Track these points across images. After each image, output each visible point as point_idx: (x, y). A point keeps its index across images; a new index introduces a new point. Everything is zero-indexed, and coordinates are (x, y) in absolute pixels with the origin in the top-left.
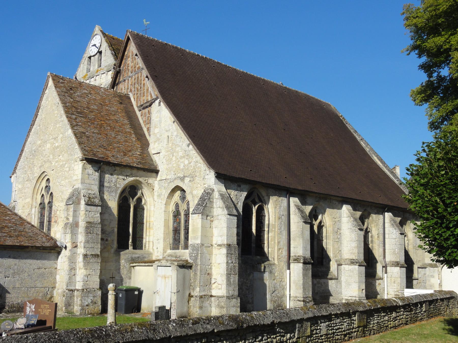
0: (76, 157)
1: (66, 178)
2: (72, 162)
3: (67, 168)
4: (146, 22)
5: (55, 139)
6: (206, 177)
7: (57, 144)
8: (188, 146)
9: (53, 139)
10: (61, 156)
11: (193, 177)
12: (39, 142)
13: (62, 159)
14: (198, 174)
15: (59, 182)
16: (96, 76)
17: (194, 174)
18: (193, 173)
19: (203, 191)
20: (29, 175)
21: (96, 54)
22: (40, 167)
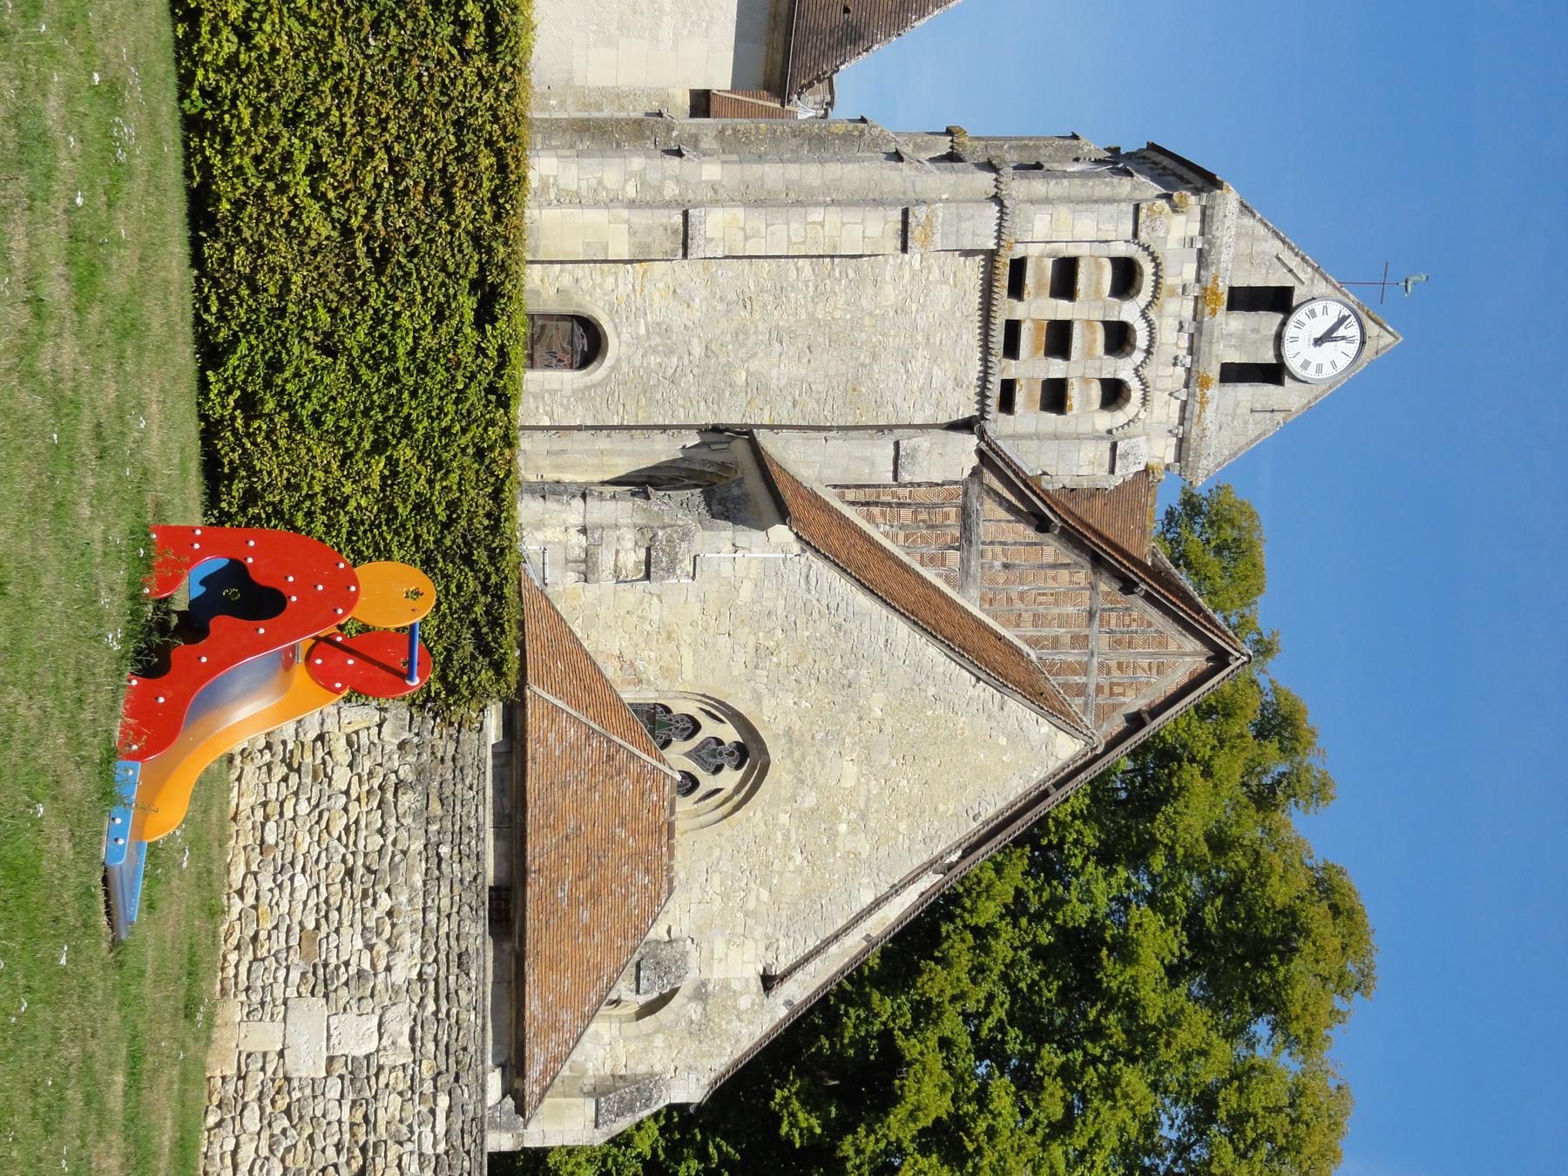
0: (782, 944)
1: (725, 897)
2: (770, 930)
3: (758, 898)
4: (1415, 284)
5: (863, 816)
6: (693, 1077)
7: (843, 828)
8: (788, 1003)
9: (868, 799)
10: (798, 858)
11: (697, 1031)
12: (877, 704)
13: (791, 867)
14: (704, 1047)
15: (719, 860)
16: (1189, 371)
17: (706, 1036)
18: (711, 1029)
19: (658, 1068)
20: (775, 659)
21: (1279, 354)
22: (789, 732)
